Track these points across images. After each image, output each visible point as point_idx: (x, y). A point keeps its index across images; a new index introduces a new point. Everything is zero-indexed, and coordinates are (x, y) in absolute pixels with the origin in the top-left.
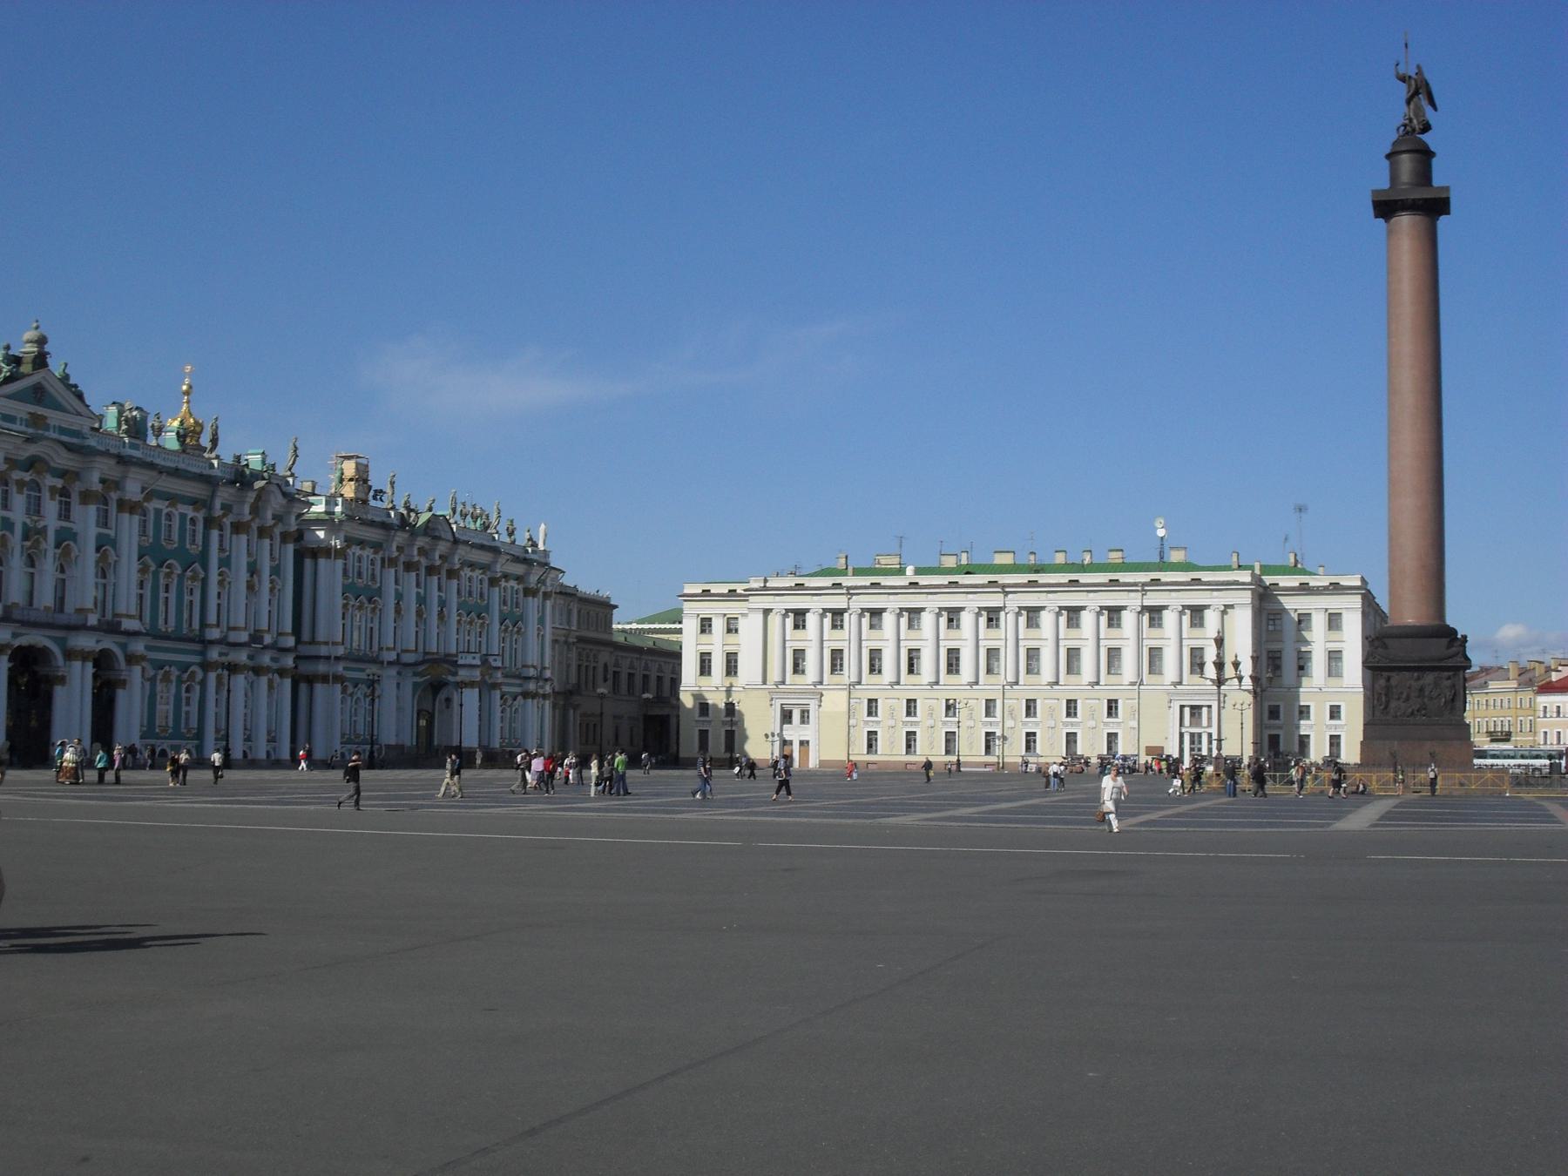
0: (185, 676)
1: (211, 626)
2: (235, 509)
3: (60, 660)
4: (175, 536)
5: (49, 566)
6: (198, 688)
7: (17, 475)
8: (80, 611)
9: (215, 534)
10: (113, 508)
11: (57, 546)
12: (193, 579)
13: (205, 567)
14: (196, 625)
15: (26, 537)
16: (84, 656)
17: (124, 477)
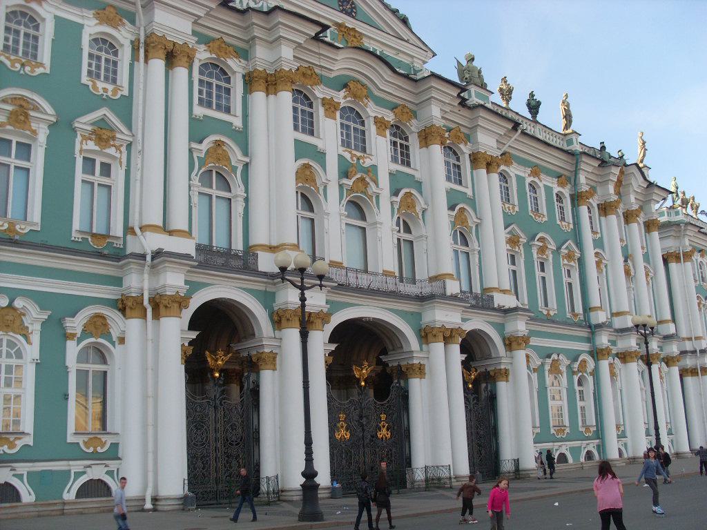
0: (576, 365)
1: (595, 309)
2: (599, 190)
3: (413, 342)
4: (543, 209)
5: (384, 217)
6: (590, 379)
7: (320, 92)
8: (433, 279)
9: (584, 209)
10: (466, 164)
11: (396, 193)
12: (569, 256)
13: (579, 244)
14: (579, 309)
15: (345, 173)
16: (448, 336)
17: (474, 128)
